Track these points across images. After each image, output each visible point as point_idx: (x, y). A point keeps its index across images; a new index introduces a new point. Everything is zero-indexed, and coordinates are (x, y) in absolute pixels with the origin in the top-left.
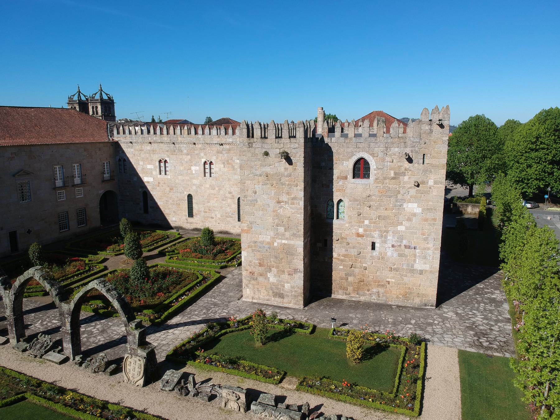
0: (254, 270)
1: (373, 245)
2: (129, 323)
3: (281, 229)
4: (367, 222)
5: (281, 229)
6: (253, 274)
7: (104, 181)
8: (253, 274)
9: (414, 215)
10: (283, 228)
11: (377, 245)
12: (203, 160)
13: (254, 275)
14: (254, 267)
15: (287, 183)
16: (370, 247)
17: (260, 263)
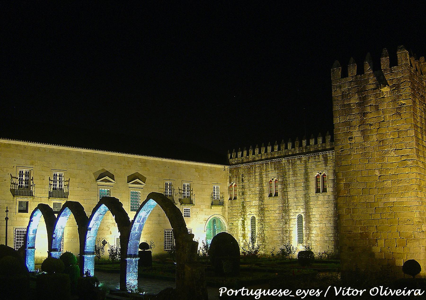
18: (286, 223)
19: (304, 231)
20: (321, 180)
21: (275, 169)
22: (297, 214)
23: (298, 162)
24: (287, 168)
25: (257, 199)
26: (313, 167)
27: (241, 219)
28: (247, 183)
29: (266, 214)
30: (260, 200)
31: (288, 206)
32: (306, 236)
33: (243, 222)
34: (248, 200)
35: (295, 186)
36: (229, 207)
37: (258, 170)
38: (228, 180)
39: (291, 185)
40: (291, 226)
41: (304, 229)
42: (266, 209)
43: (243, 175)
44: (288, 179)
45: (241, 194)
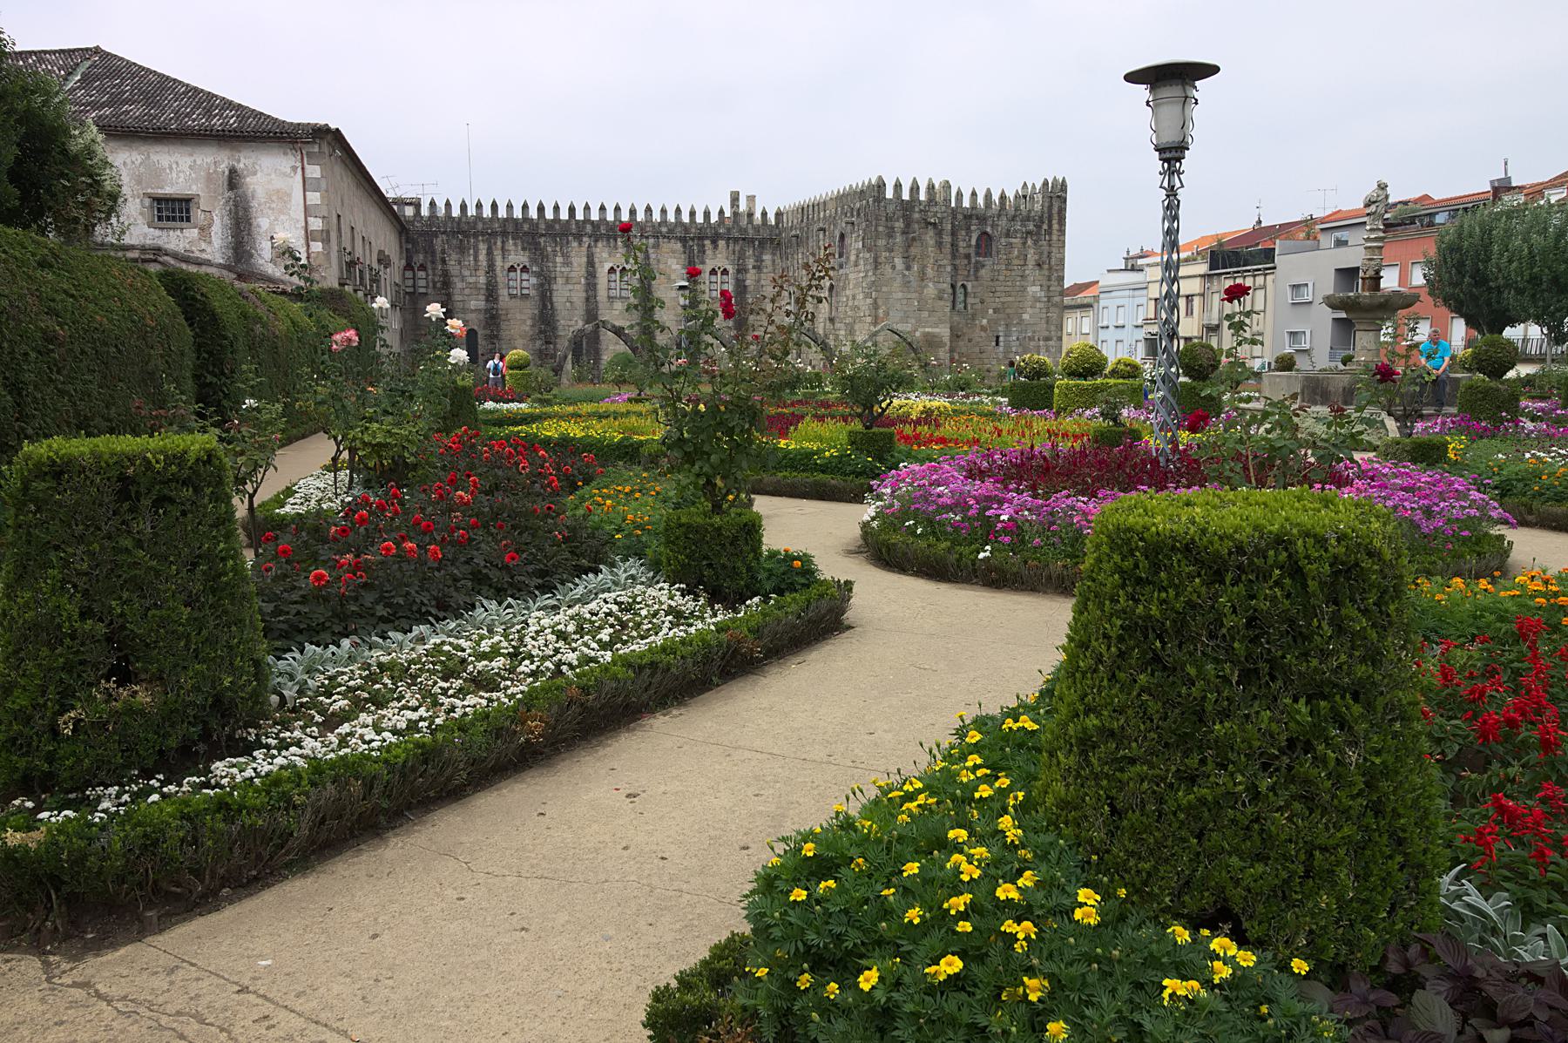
1: (998, 337)
4: (991, 311)
9: (1038, 300)
11: (1001, 339)
12: (607, 266)
18: (548, 343)
21: (524, 249)
23: (575, 244)
24: (549, 249)
25: (483, 298)
26: (605, 255)
29: (503, 326)
30: (487, 300)
31: (553, 315)
34: (457, 298)
35: (568, 280)
37: (483, 247)
39: (560, 281)
42: (503, 317)
43: (443, 252)
45: (439, 285)
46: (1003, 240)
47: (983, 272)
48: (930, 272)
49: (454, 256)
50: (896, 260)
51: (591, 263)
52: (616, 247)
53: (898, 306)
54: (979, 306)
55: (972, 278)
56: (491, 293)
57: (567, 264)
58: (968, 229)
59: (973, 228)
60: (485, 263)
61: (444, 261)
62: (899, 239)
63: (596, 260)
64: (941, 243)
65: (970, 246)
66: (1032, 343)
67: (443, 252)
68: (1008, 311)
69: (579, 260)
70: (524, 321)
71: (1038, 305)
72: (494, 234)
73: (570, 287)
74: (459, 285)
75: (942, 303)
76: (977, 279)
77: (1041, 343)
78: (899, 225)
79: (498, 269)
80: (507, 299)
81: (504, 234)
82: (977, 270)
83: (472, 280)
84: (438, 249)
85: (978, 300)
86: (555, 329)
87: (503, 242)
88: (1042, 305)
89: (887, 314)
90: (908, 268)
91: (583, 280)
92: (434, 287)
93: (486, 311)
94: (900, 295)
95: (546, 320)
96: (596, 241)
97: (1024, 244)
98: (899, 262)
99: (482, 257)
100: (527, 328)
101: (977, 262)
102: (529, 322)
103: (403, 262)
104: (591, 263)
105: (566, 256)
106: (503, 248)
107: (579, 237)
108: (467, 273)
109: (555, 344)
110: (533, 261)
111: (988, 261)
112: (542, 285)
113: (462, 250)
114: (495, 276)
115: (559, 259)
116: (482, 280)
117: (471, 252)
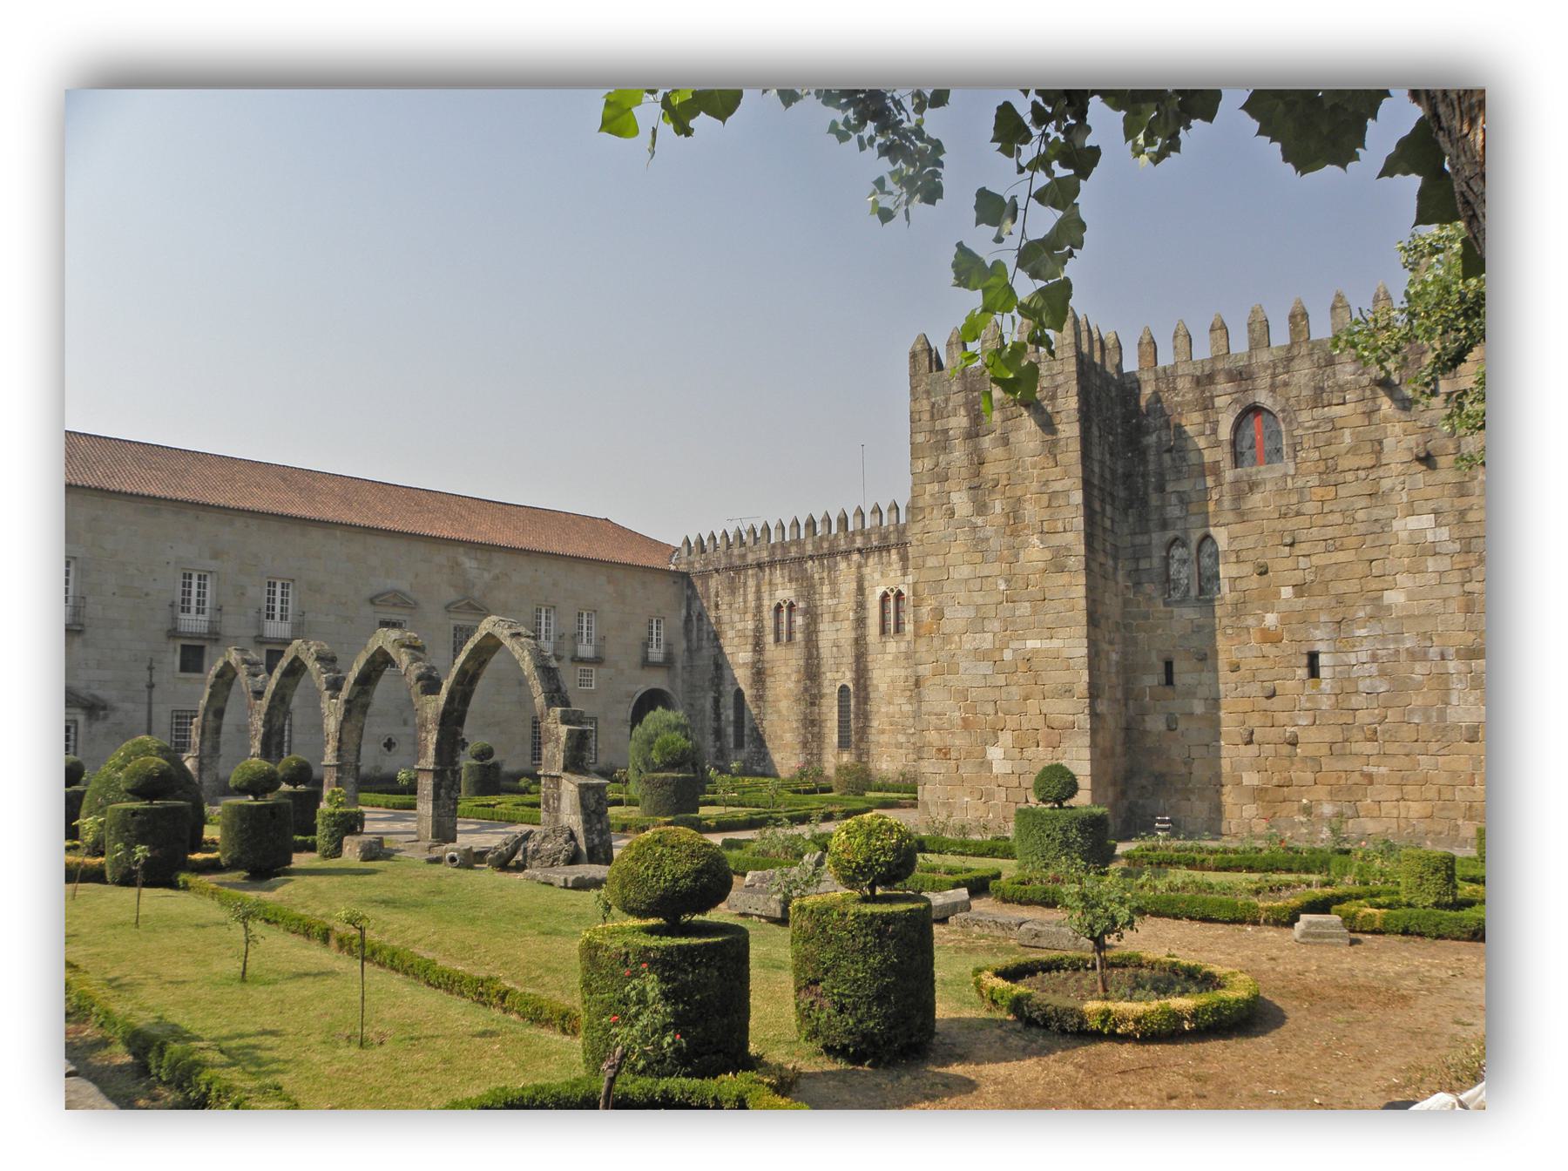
0: (949, 740)
1: (1313, 658)
2: (548, 709)
3: (1024, 609)
4: (1287, 592)
5: (1024, 609)
6: (945, 754)
7: (646, 663)
8: (945, 754)
10: (1028, 604)
11: (1323, 660)
12: (880, 591)
13: (948, 757)
14: (949, 733)
15: (1036, 472)
16: (1302, 672)
17: (964, 719)
18: (813, 704)
19: (852, 723)
20: (892, 604)
21: (790, 580)
22: (839, 685)
23: (843, 565)
24: (816, 576)
25: (749, 647)
26: (877, 576)
27: (712, 694)
28: (728, 612)
29: (769, 682)
30: (755, 651)
31: (818, 666)
32: (857, 733)
33: (717, 701)
34: (727, 650)
36: (684, 668)
37: (751, 583)
38: (684, 604)
39: (826, 617)
40: (824, 709)
41: (852, 716)
42: (769, 672)
43: (717, 596)
44: (818, 603)
46: (1304, 416)
47: (1256, 500)
48: (1032, 511)
49: (727, 599)
50: (955, 497)
51: (861, 590)
52: (890, 564)
53: (962, 596)
54: (1254, 582)
55: (1230, 517)
56: (758, 646)
57: (834, 593)
58: (1207, 406)
59: (1219, 402)
60: (753, 604)
61: (717, 606)
62: (959, 454)
63: (866, 584)
64: (1055, 443)
65: (1217, 444)
66: (1419, 668)
67: (717, 596)
68: (1341, 587)
69: (848, 587)
70: (788, 676)
71: (1431, 564)
72: (760, 566)
73: (838, 625)
74: (730, 634)
75: (1063, 579)
76: (1242, 516)
77: (1453, 666)
78: (959, 422)
79: (765, 609)
80: (773, 648)
81: (772, 564)
82: (1238, 497)
83: (740, 626)
84: (712, 591)
85: (1247, 569)
86: (820, 686)
87: (771, 574)
88: (1445, 563)
89: (939, 614)
90: (981, 508)
91: (851, 615)
92: (708, 638)
93: (754, 664)
94: (965, 571)
95: (812, 672)
96: (868, 557)
97: (1369, 414)
98: (961, 501)
99: (751, 597)
100: (791, 685)
101: (1236, 482)
102: (794, 677)
103: (684, 612)
104: (861, 590)
105: (833, 583)
106: (770, 583)
107: (847, 554)
108: (736, 617)
109: (820, 706)
110: (799, 596)
111: (1268, 474)
112: (807, 626)
113: (733, 591)
114: (761, 621)
115: (826, 589)
116: (750, 625)
117: (741, 591)
